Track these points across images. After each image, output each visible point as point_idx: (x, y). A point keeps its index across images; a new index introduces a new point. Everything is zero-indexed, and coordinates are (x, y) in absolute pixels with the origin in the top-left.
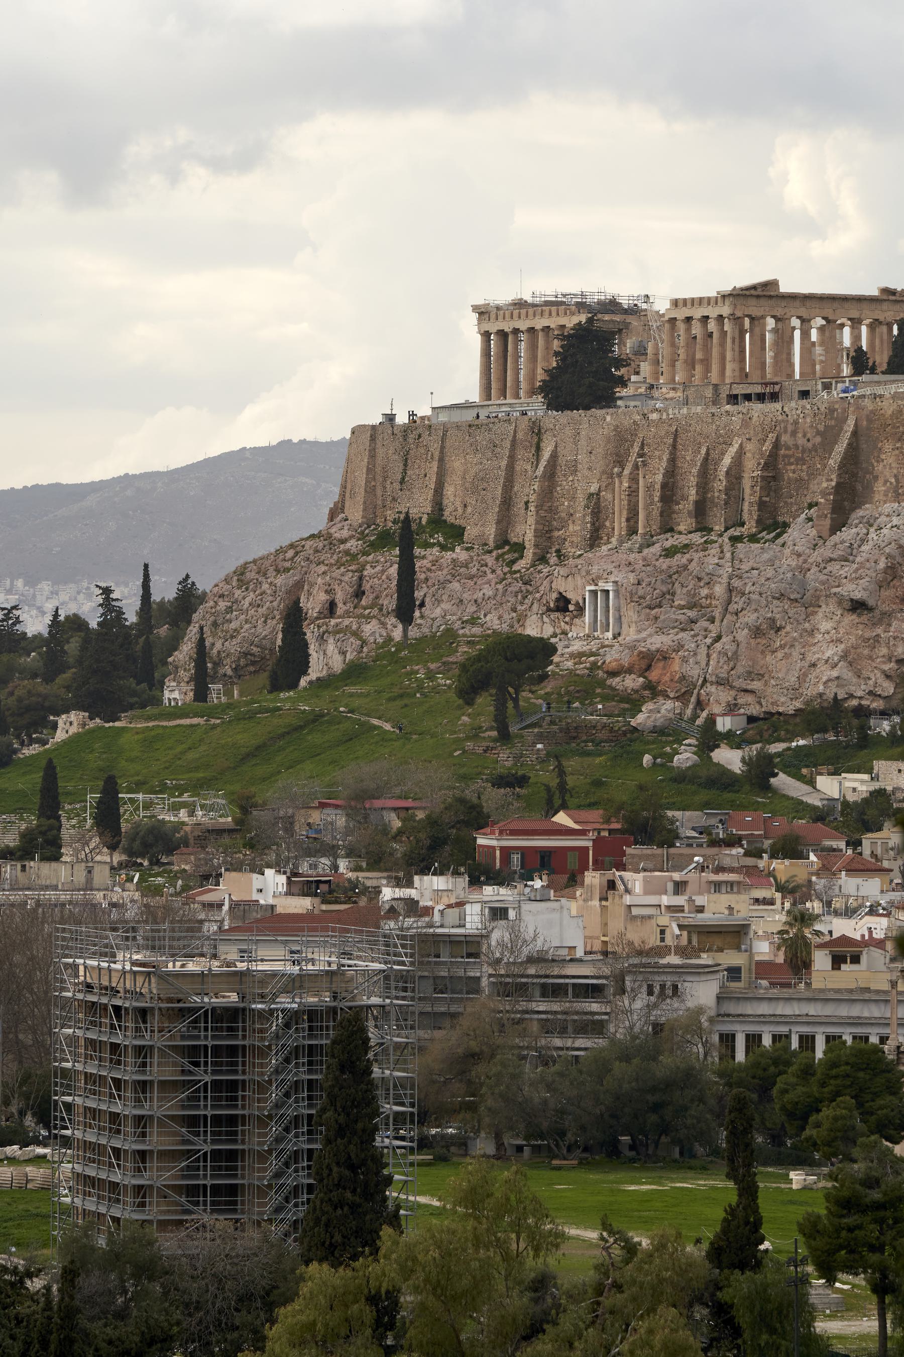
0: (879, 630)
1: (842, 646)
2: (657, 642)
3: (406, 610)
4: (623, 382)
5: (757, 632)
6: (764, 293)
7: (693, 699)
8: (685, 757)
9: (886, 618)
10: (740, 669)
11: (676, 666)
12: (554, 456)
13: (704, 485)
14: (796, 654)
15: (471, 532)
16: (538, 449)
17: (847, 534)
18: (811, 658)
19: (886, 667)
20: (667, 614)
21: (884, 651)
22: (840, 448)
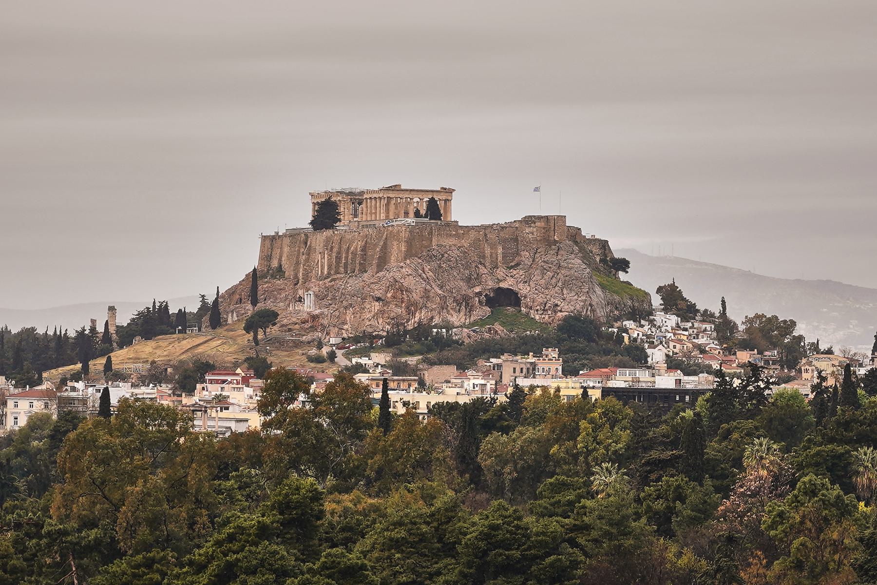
2: (317, 312)
3: (254, 302)
4: (340, 220)
6: (395, 188)
8: (313, 352)
11: (321, 321)
12: (310, 246)
13: (347, 258)
14: (358, 316)
15: (287, 274)
16: (306, 243)
17: (380, 274)
18: (362, 318)
20: (324, 302)
22: (382, 243)
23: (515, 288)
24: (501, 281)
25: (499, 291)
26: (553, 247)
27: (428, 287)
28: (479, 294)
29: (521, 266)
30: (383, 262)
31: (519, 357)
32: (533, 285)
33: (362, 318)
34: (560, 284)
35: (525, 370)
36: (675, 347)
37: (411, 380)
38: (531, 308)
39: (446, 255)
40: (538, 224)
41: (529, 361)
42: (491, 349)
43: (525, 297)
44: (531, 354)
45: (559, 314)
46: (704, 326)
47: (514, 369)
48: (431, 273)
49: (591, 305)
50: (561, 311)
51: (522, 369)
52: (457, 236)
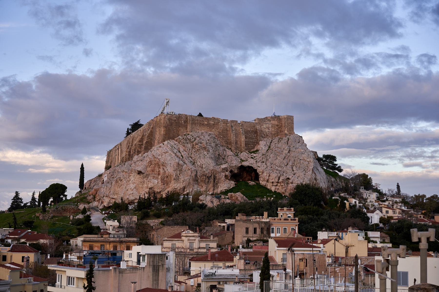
0: (145, 179)
1: (135, 185)
5: (117, 182)
7: (101, 201)
9: (147, 176)
10: (112, 192)
14: (124, 187)
19: (146, 190)
21: (146, 185)
23: (255, 166)
24: (244, 161)
25: (242, 168)
26: (284, 138)
27: (181, 162)
28: (225, 170)
29: (260, 151)
30: (149, 146)
31: (254, 217)
32: (268, 164)
33: (127, 188)
34: (290, 164)
35: (258, 231)
36: (387, 212)
37: (130, 242)
38: (268, 181)
39: (198, 139)
40: (273, 122)
41: (264, 220)
42: (228, 212)
43: (263, 173)
44: (266, 214)
45: (291, 185)
46: (395, 199)
47: (247, 229)
48: (185, 152)
49: (316, 179)
50: (292, 183)
51: (255, 229)
52: (208, 125)
